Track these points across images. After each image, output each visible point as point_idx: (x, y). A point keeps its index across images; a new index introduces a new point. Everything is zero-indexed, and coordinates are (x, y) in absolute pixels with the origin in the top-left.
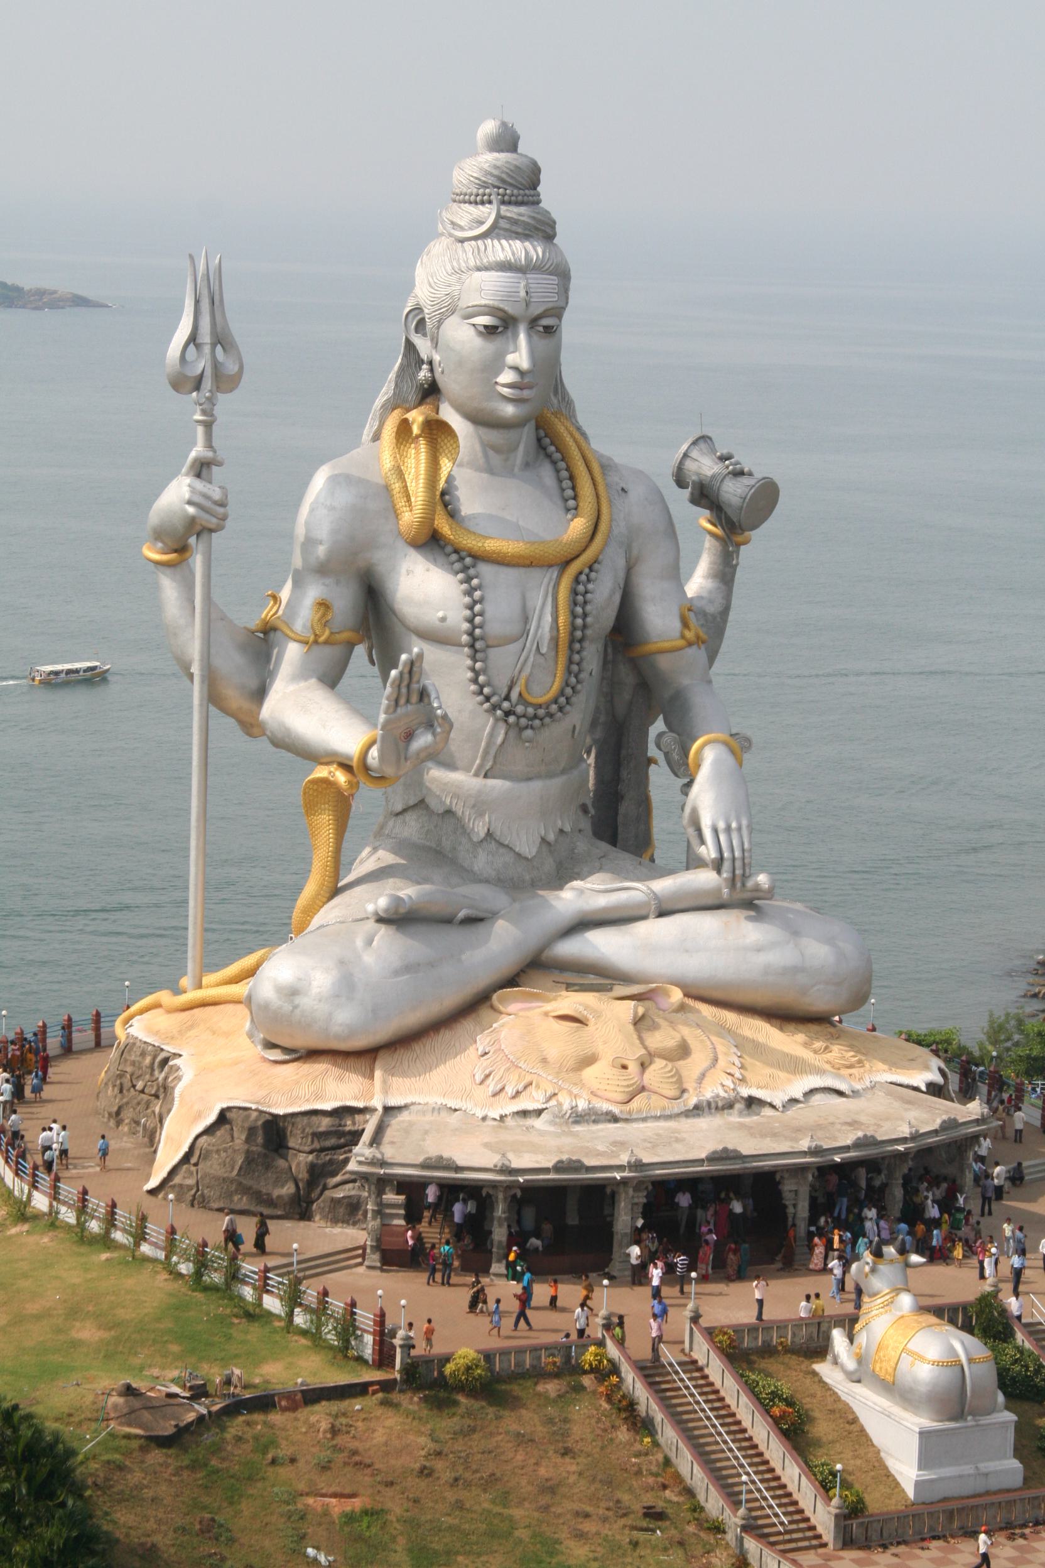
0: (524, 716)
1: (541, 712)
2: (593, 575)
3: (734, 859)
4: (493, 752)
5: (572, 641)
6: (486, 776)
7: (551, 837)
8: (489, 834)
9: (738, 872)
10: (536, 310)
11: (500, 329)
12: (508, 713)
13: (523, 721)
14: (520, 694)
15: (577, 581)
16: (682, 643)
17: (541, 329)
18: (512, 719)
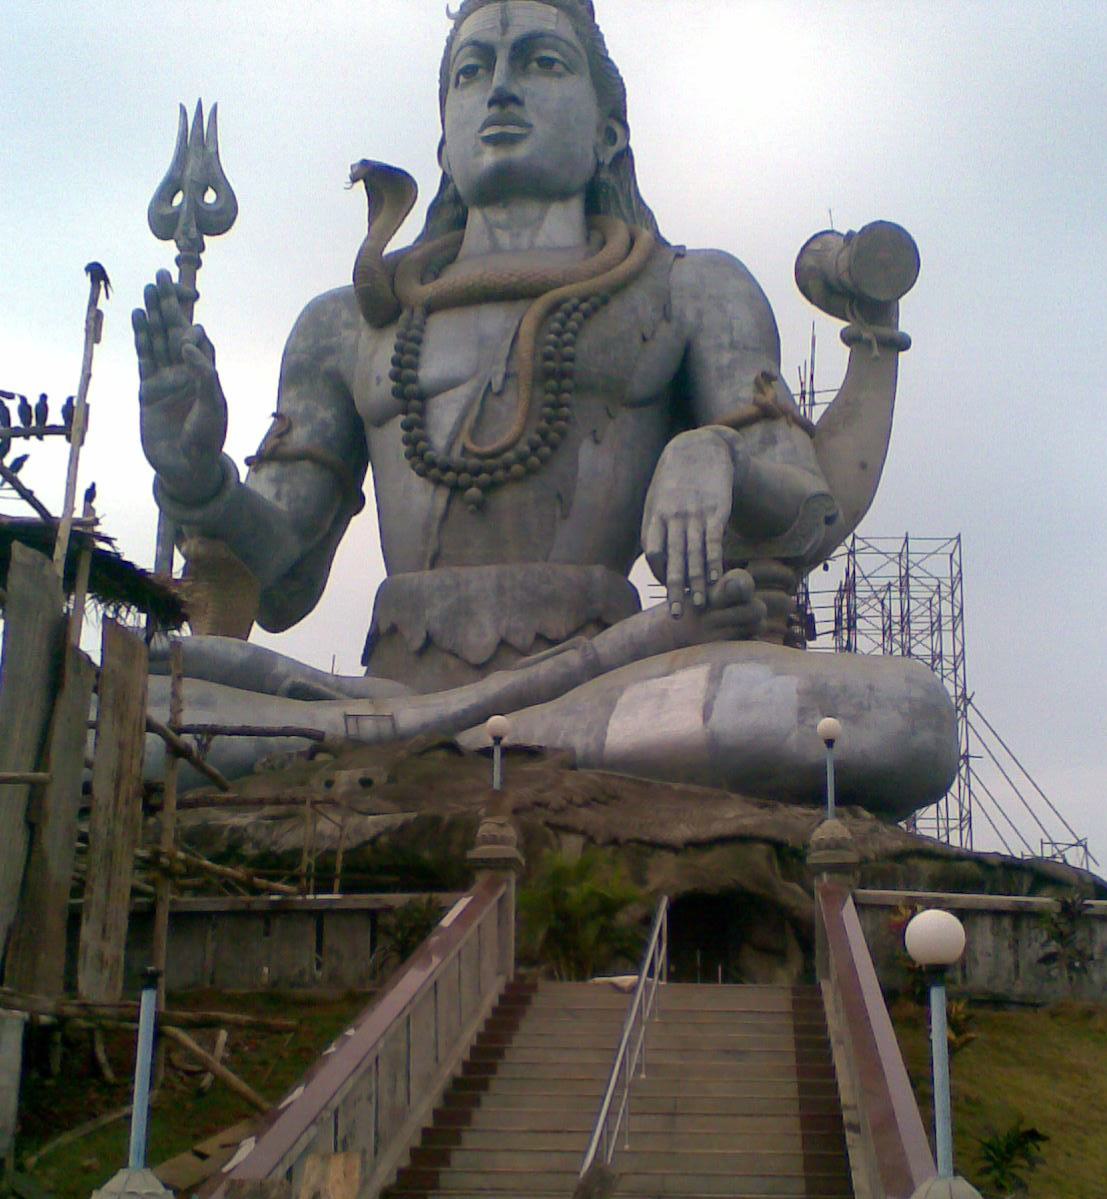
0: (464, 469)
1: (490, 462)
2: (584, 306)
3: (685, 555)
4: (435, 528)
5: (542, 376)
6: (433, 566)
7: (517, 640)
8: (429, 641)
9: (695, 570)
10: (514, 34)
11: (480, 71)
12: (446, 469)
13: (465, 477)
14: (465, 451)
15: (555, 307)
16: (752, 410)
17: (534, 65)
18: (450, 476)
